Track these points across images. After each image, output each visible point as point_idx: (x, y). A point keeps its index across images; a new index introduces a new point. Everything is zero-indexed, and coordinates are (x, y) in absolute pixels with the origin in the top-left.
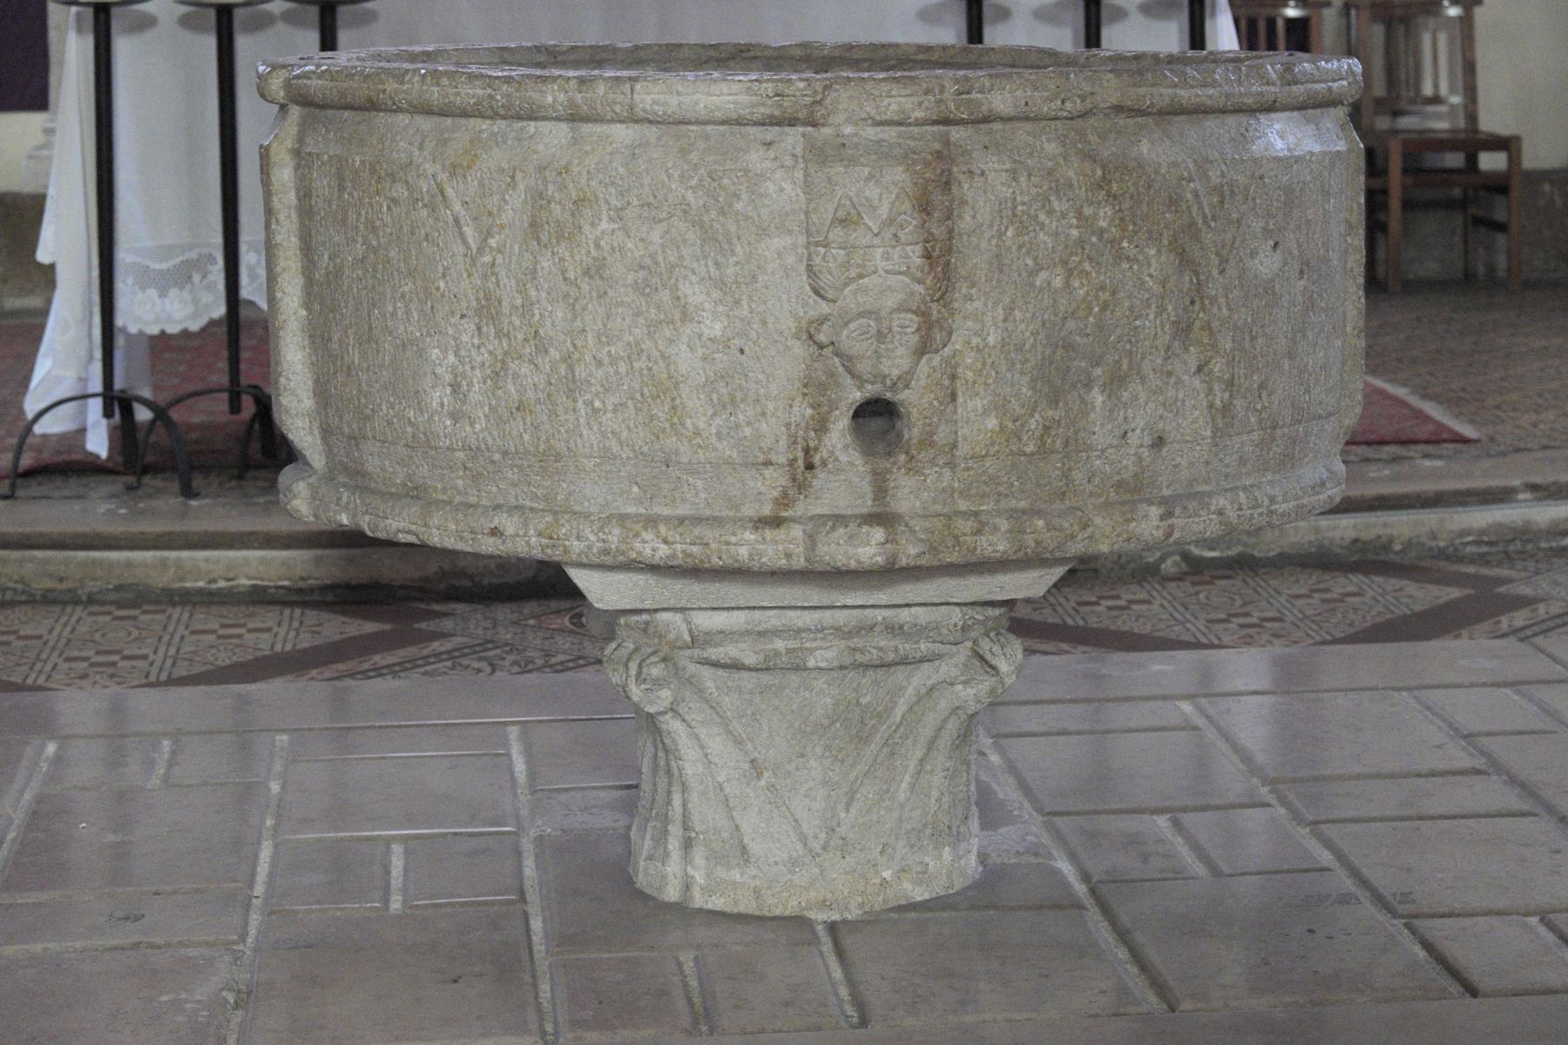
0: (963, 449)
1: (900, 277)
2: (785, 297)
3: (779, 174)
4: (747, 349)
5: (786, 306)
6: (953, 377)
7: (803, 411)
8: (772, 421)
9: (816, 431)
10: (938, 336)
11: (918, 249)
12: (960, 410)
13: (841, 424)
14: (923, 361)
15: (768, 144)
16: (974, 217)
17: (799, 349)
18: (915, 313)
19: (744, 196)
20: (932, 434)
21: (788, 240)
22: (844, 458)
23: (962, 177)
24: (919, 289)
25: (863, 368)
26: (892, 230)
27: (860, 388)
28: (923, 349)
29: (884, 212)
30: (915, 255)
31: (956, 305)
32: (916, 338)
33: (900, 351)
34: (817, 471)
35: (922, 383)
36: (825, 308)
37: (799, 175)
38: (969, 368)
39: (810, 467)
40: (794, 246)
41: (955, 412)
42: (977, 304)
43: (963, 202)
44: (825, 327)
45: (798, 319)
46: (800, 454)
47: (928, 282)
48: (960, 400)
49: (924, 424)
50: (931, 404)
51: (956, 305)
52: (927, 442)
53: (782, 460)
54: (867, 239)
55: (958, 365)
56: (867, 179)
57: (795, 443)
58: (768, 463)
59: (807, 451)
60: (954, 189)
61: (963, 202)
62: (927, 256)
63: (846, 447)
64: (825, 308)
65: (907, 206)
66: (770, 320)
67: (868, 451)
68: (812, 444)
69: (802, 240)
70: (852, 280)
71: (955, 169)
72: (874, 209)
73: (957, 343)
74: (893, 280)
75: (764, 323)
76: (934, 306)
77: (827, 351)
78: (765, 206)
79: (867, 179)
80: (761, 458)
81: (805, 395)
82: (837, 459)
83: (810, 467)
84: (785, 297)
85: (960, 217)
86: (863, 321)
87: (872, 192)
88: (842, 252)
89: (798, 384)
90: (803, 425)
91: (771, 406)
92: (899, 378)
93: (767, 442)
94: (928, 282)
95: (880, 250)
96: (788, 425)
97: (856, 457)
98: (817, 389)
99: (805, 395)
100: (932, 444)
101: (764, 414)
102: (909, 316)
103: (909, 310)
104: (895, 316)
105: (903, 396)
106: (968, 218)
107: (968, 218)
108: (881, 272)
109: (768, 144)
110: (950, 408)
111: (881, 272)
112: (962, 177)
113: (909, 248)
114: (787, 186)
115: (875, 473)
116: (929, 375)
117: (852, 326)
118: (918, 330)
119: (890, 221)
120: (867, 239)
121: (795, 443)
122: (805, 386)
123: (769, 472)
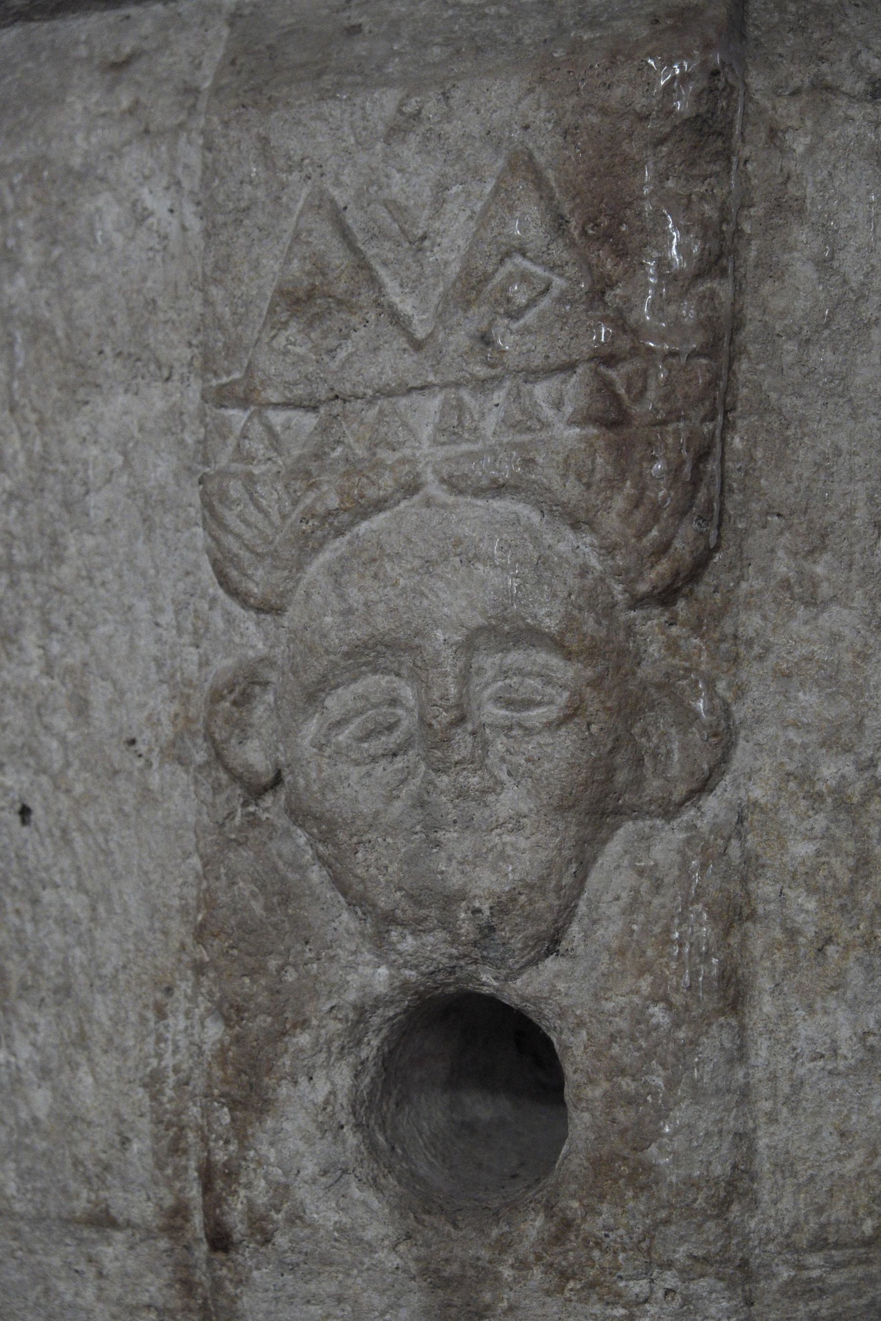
0: (779, 1207)
1: (502, 505)
2: (142, 607)
3: (136, 159)
4: (38, 813)
5: (147, 645)
6: (735, 915)
7: (196, 1032)
8: (107, 1063)
9: (234, 1105)
10: (680, 754)
11: (575, 389)
12: (761, 1051)
13: (316, 1092)
14: (615, 847)
15: (118, 67)
16: (824, 265)
17: (183, 798)
18: (556, 644)
19: (31, 255)
20: (642, 1137)
21: (157, 399)
22: (325, 1214)
23: (787, 111)
24: (574, 547)
25: (380, 865)
26: (476, 318)
27: (380, 943)
28: (597, 806)
29: (453, 238)
30: (559, 411)
31: (751, 623)
32: (564, 745)
33: (511, 800)
34: (245, 1256)
35: (610, 932)
36: (253, 637)
37: (192, 155)
38: (808, 878)
39: (220, 1241)
40: (176, 413)
41: (740, 1055)
42: (840, 619)
43: (785, 207)
44: (260, 712)
45: (181, 691)
46: (194, 1192)
47: (611, 522)
48: (765, 1005)
49: (611, 1100)
50: (639, 1017)
51: (751, 623)
52: (624, 1169)
53: (140, 1206)
54: (391, 362)
55: (752, 865)
56: (396, 132)
57: (177, 1148)
58: (103, 1221)
59: (208, 1175)
60: (750, 148)
61: (785, 207)
62: (610, 416)
63: (334, 1173)
64: (253, 637)
65: (527, 222)
66: (100, 694)
67: (421, 1204)
68: (220, 1157)
69: (192, 395)
70: (333, 523)
71: (757, 81)
72: (419, 243)
73: (755, 775)
74: (473, 516)
75: (81, 708)
76: (651, 624)
77: (271, 807)
78: (83, 282)
79: (396, 132)
80: (82, 1202)
81: (199, 968)
82: (296, 1218)
83: (220, 1241)
84: (142, 607)
85: (773, 270)
86: (374, 683)
87: (411, 176)
88: (309, 421)
89: (180, 931)
90: (199, 1083)
91: (102, 1009)
92: (501, 908)
93: (92, 1145)
94: (611, 522)
95: (433, 404)
96: (153, 1082)
97: (367, 1212)
98: (239, 946)
99: (199, 968)
100: (643, 1177)
101: (82, 1041)
102: (543, 658)
103: (529, 636)
104: (488, 662)
105: (540, 987)
106: (804, 272)
107: (804, 272)
108: (434, 489)
109: (118, 67)
110: (716, 1040)
111: (434, 489)
112: (787, 111)
113: (541, 390)
114: (156, 201)
115: (435, 1277)
116: (634, 905)
117: (335, 703)
118: (573, 713)
119: (471, 287)
120: (391, 362)
121: (177, 1148)
122: (201, 933)
123: (113, 1252)
